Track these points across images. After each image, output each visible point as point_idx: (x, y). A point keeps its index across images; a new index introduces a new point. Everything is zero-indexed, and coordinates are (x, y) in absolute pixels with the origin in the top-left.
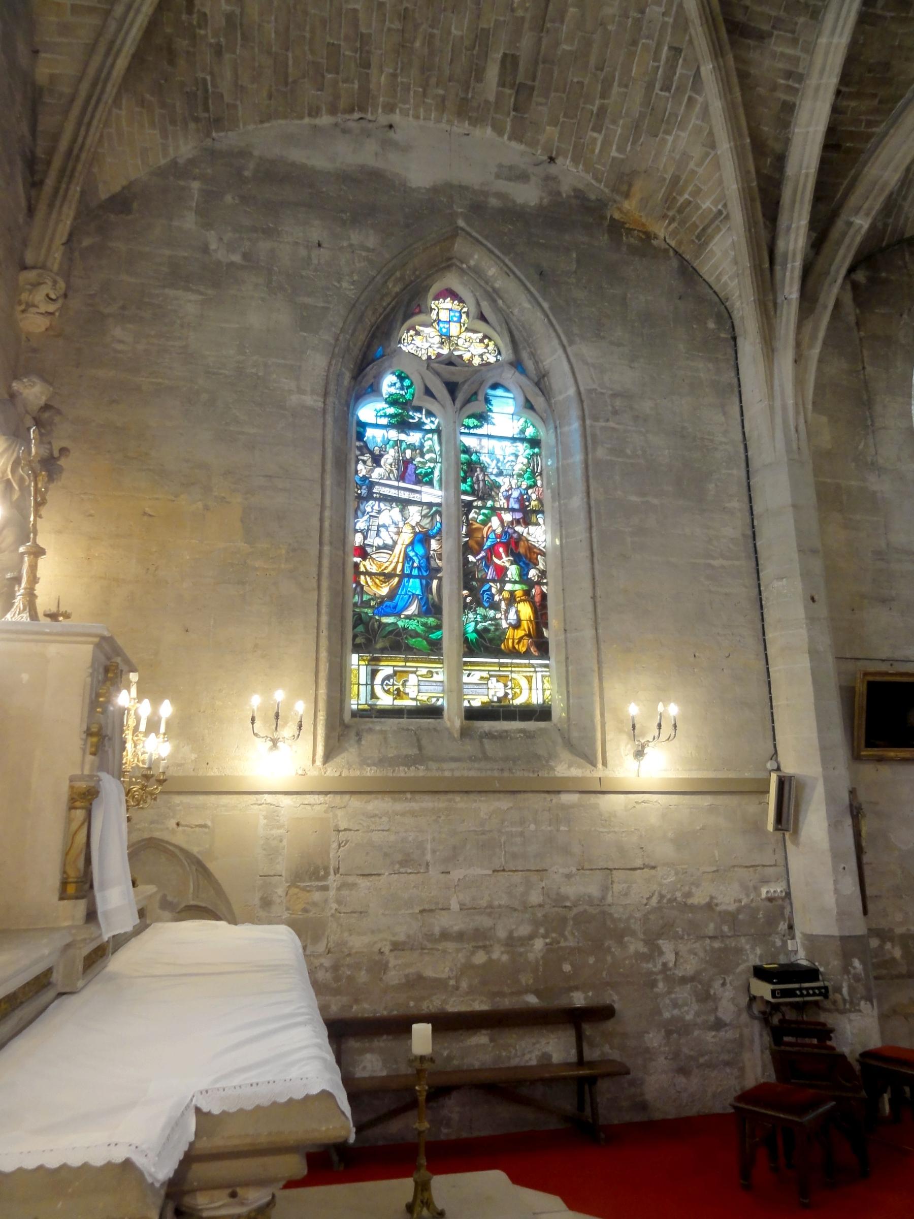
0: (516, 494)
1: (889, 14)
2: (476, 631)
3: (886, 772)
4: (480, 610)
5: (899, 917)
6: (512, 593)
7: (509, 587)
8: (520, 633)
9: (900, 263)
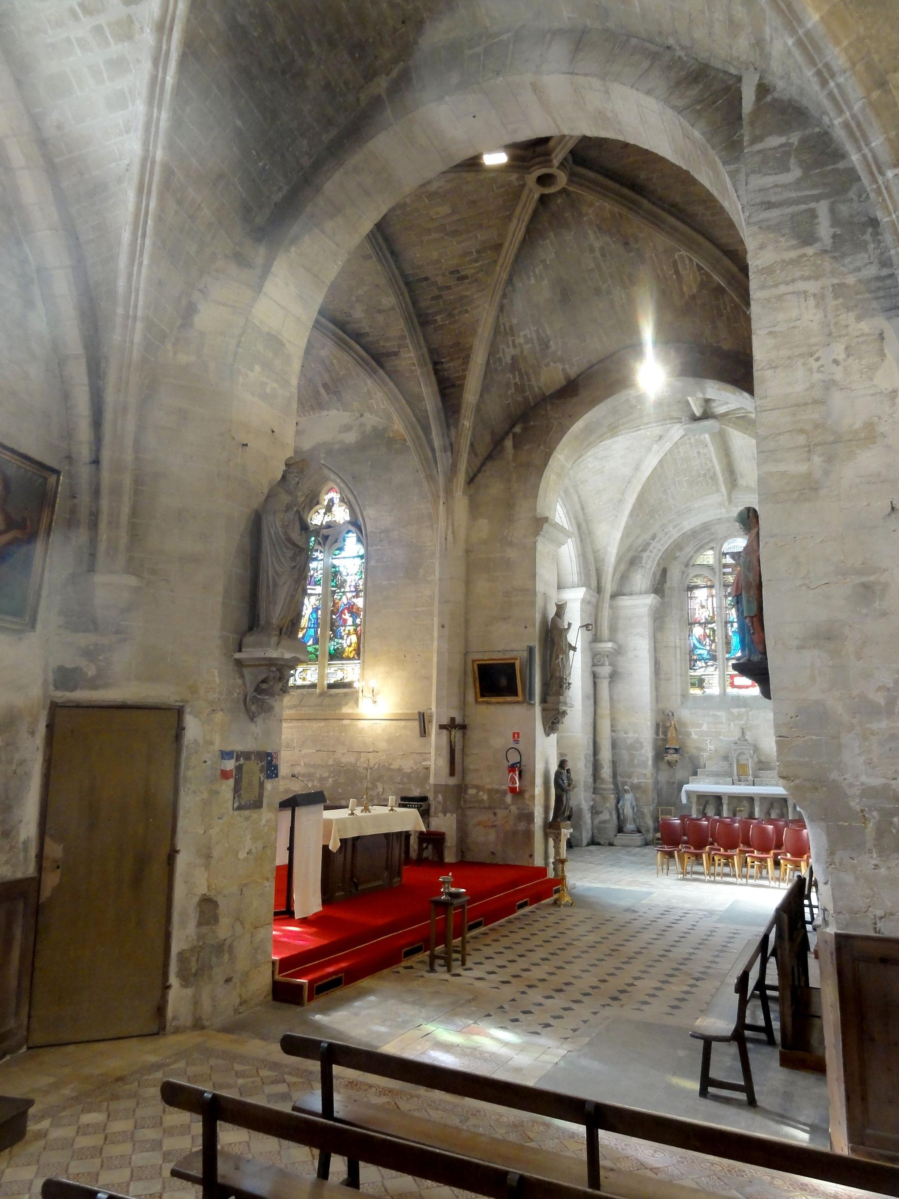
0: (353, 584)
1: (447, 322)
2: (334, 649)
3: (492, 709)
4: (336, 640)
5: (488, 780)
6: (349, 631)
7: (348, 628)
8: (351, 649)
9: (544, 413)
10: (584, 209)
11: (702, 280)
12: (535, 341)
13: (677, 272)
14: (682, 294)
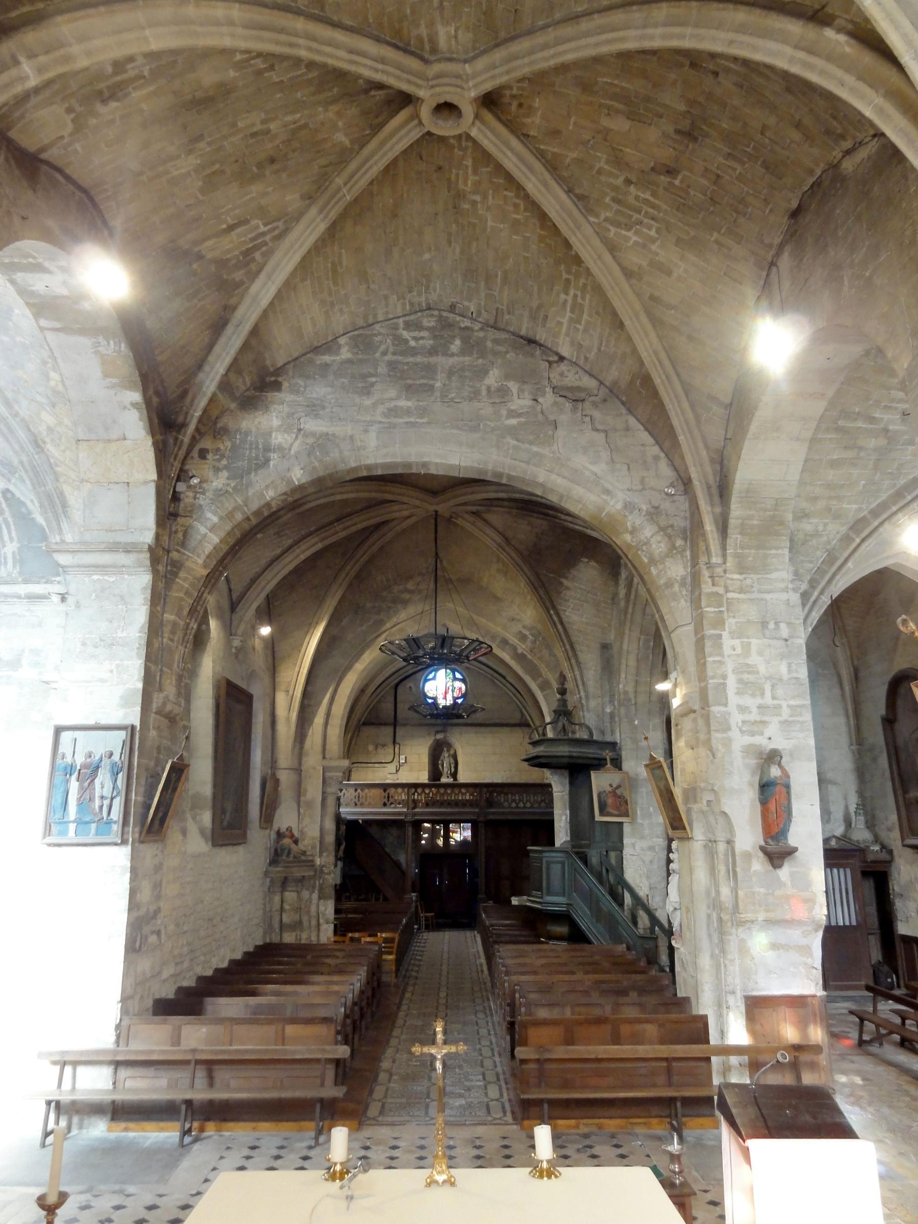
10: (334, 108)
11: (228, 260)
12: (118, 78)
13: (231, 228)
14: (196, 243)
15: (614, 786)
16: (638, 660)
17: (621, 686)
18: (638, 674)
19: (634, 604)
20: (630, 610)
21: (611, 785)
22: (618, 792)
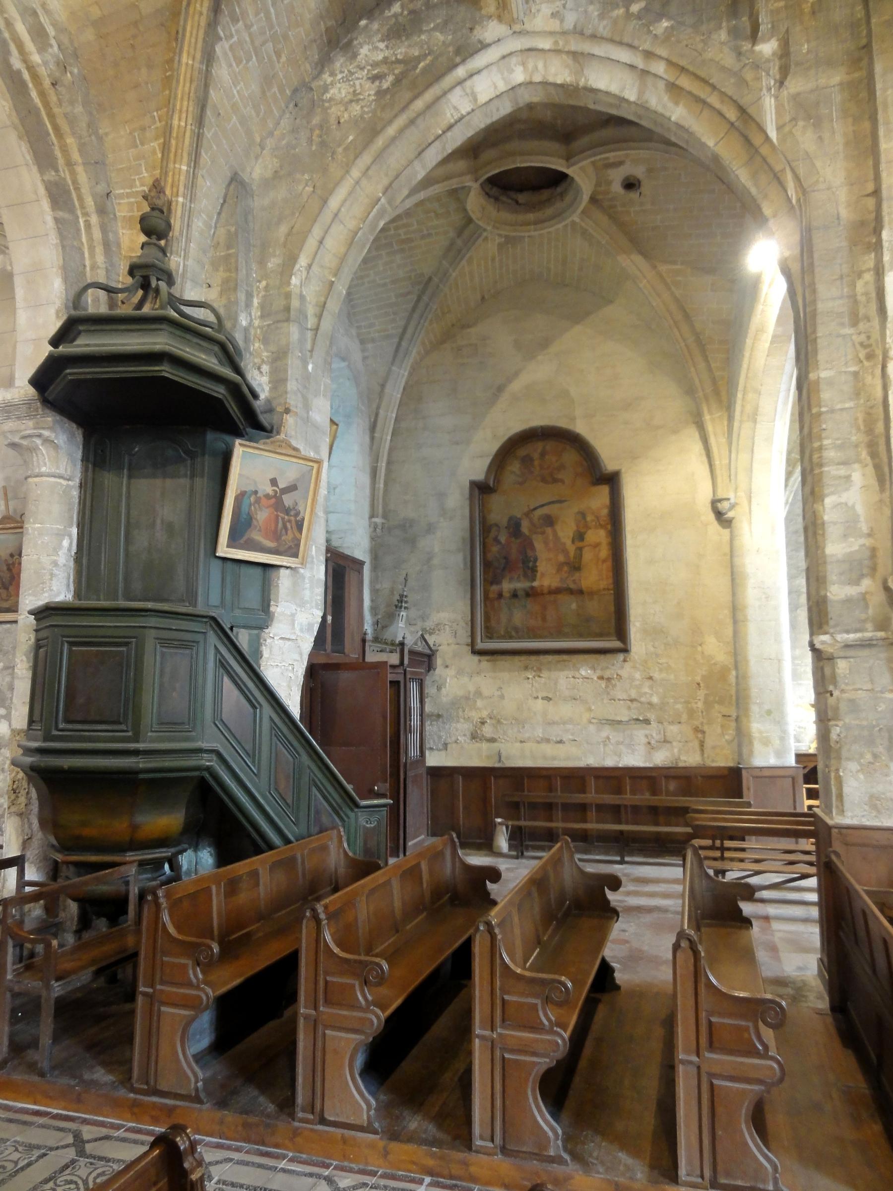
15: (282, 485)
16: (351, 244)
17: (294, 280)
18: (336, 273)
19: (412, 122)
20: (391, 131)
21: (274, 482)
22: (288, 500)
